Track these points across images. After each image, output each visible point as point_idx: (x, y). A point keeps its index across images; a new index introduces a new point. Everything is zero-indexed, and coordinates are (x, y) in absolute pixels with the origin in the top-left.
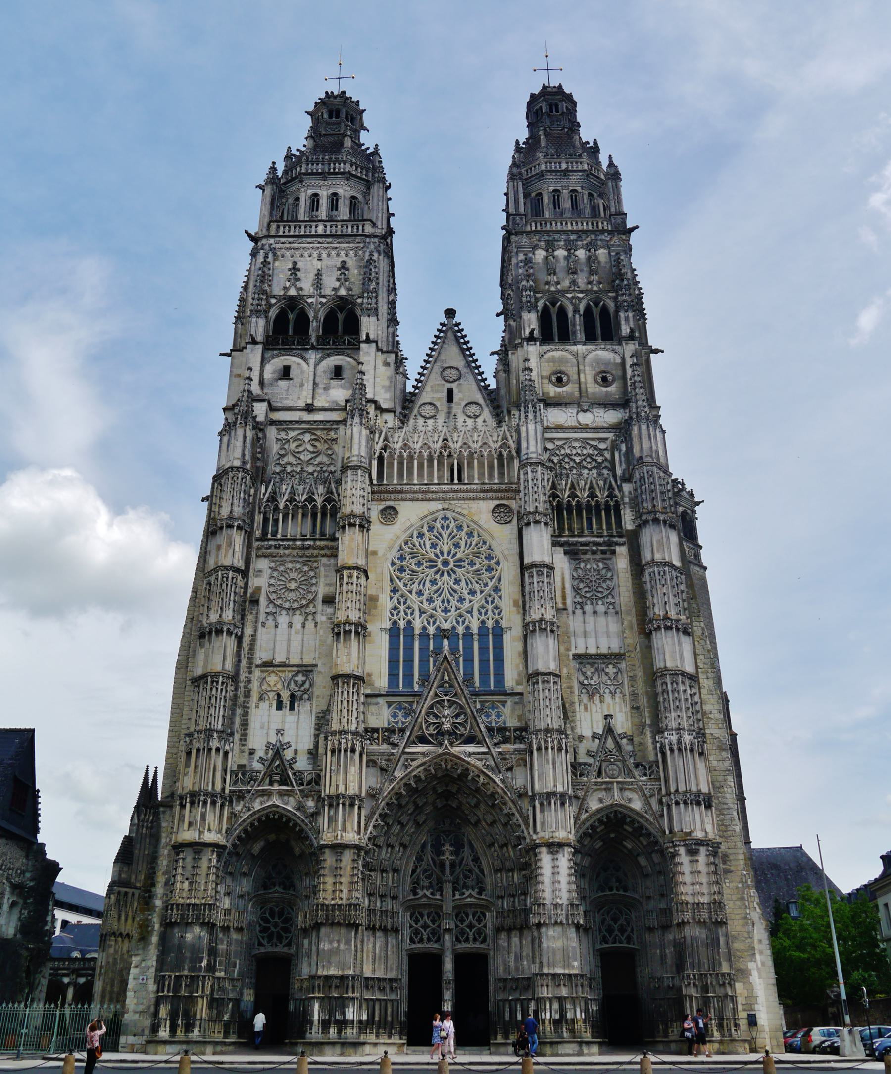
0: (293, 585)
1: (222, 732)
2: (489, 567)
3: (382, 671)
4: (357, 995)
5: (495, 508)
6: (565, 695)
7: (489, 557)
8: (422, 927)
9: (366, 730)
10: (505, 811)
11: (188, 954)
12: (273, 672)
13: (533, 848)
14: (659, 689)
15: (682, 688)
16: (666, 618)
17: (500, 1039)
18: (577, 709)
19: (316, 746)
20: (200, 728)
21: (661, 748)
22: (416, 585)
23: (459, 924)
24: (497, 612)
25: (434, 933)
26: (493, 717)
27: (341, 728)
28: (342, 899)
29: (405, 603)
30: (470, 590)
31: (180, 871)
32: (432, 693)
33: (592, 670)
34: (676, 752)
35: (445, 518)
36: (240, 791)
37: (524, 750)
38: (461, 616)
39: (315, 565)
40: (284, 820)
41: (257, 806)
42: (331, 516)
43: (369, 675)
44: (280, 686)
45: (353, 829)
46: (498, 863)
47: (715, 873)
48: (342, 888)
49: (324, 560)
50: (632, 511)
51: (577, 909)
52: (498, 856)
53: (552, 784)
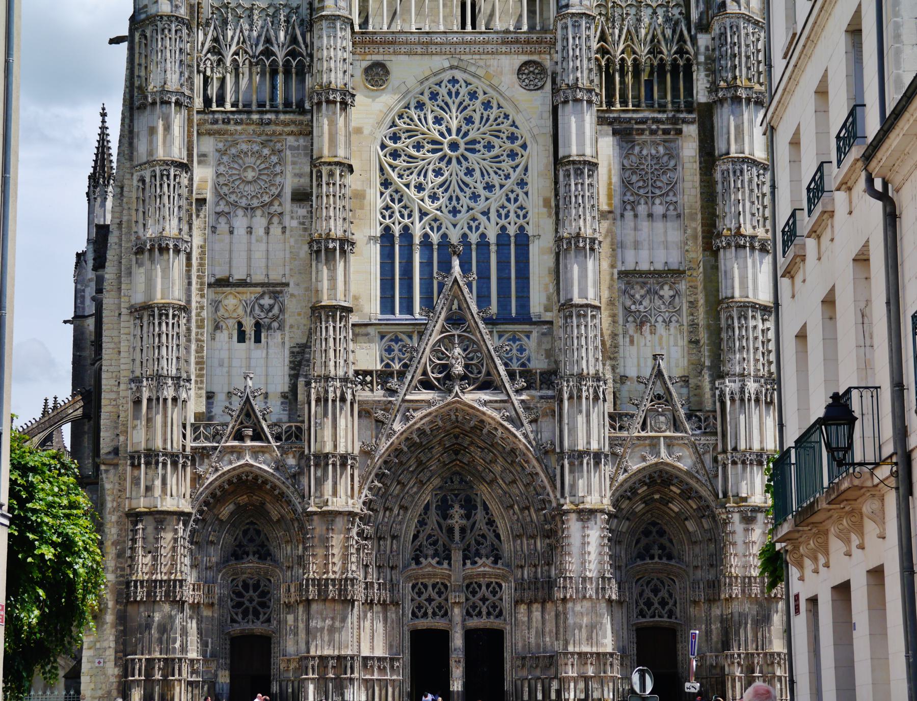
0: (250, 175)
2: (512, 151)
5: (521, 66)
7: (512, 138)
8: (426, 600)
9: (357, 373)
10: (528, 470)
14: (723, 323)
16: (738, 234)
18: (621, 343)
19: (294, 389)
21: (720, 396)
22: (414, 176)
23: (470, 596)
24: (521, 213)
25: (440, 607)
26: (514, 351)
27: (327, 373)
28: (334, 572)
29: (400, 201)
30: (487, 183)
34: (738, 402)
35: (454, 81)
36: (204, 448)
37: (553, 397)
38: (474, 219)
39: (278, 146)
40: (260, 481)
42: (297, 74)
44: (240, 311)
48: (336, 560)
49: (291, 140)
50: (707, 76)
52: (518, 520)
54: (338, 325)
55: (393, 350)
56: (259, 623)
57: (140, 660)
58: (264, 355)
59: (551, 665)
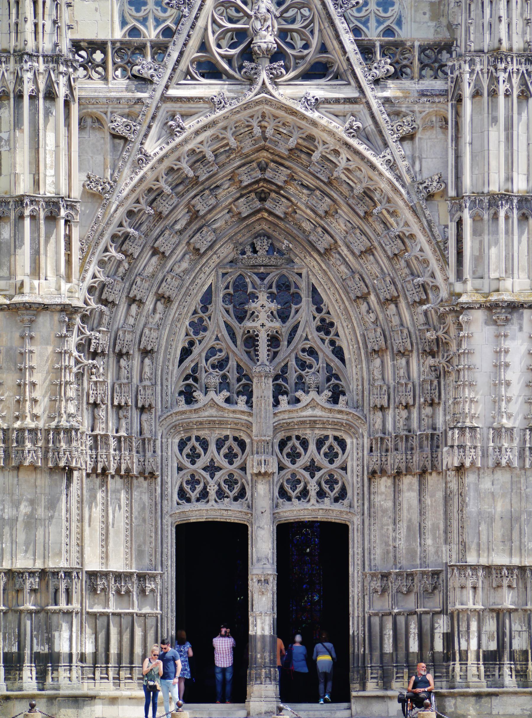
4: (75, 606)
9: (76, 46)
10: (397, 229)
23: (287, 462)
25: (231, 482)
27: (20, 46)
28: (35, 417)
37: (444, 93)
48: (37, 394)
52: (376, 322)
59: (435, 588)
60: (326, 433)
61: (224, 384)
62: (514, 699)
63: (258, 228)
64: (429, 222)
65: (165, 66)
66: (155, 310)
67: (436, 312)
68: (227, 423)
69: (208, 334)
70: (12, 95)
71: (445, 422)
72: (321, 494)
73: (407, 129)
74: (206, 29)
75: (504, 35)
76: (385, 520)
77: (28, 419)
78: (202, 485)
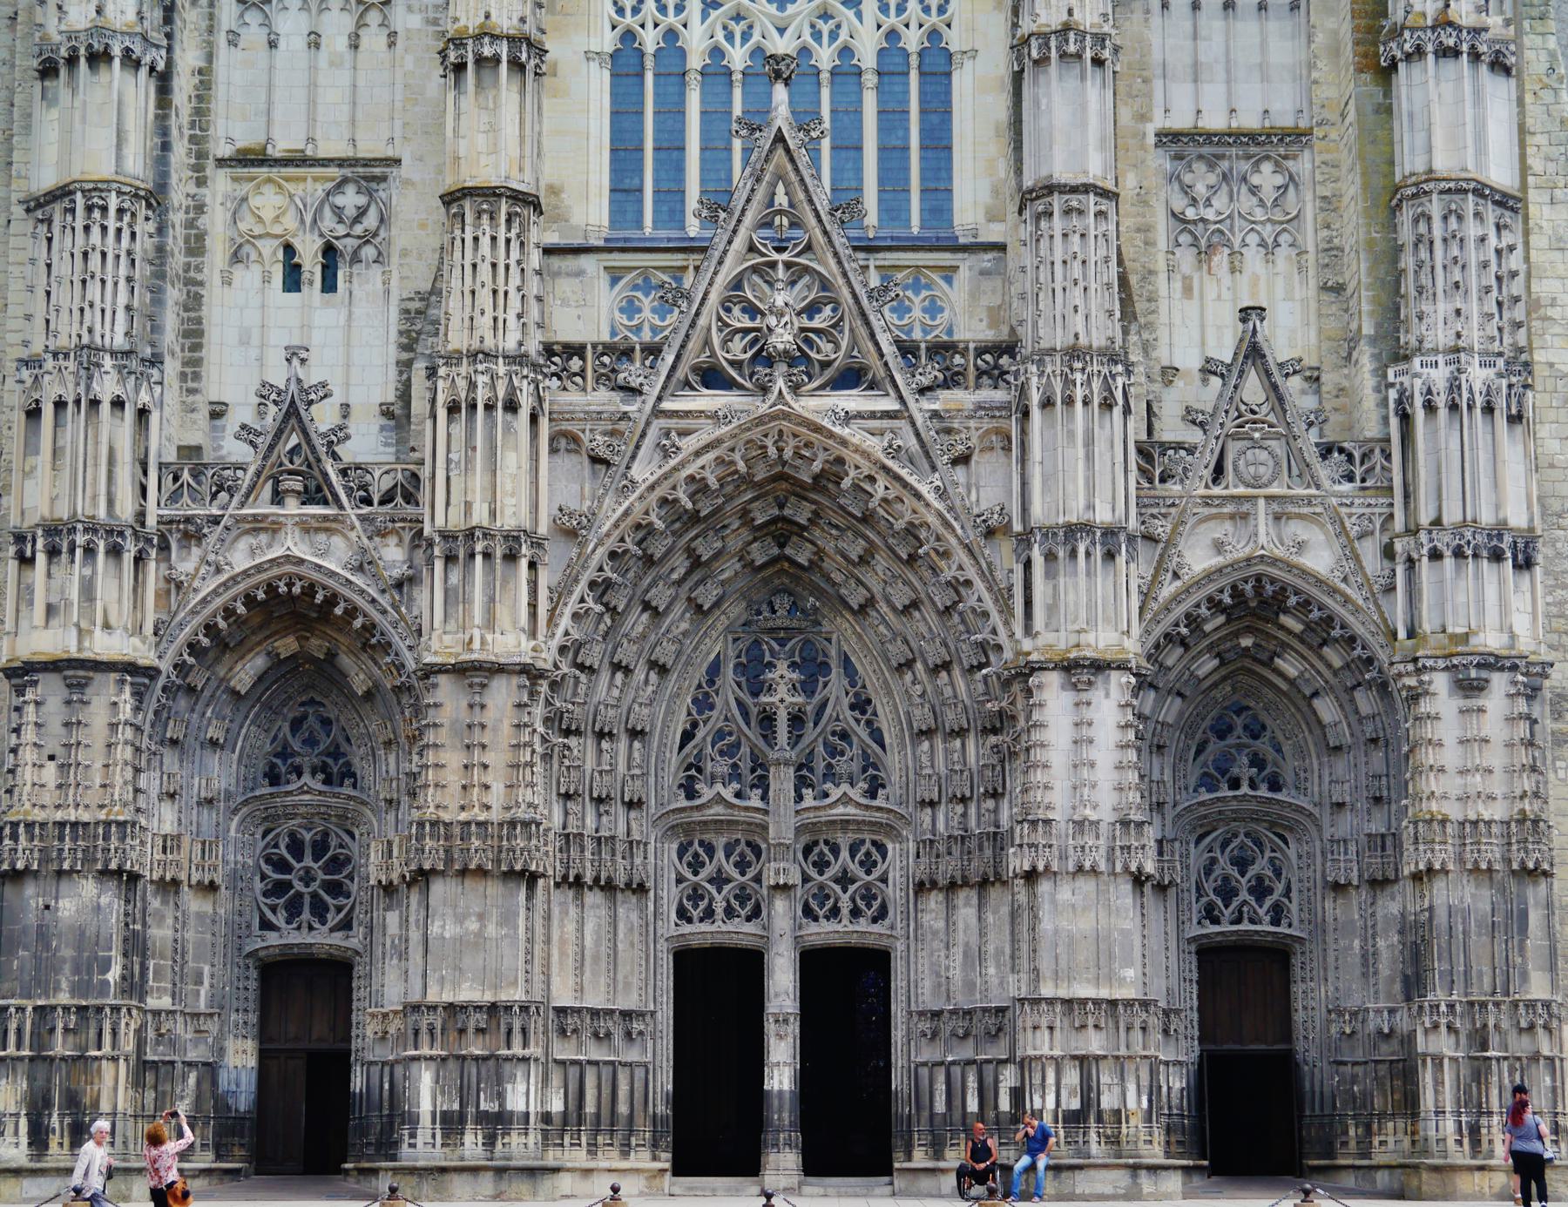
1: (127, 354)
3: (593, 178)
4: (535, 1050)
6: (1128, 253)
9: (549, 350)
10: (948, 574)
11: (67, 952)
12: (269, 180)
13: (1025, 672)
14: (1406, 234)
15: (1472, 230)
17: (920, 1158)
18: (1163, 291)
19: (405, 395)
20: (62, 342)
21: (1399, 402)
23: (813, 873)
25: (742, 898)
26: (917, 313)
27: (476, 345)
28: (488, 808)
31: (29, 735)
32: (739, 243)
33: (1212, 179)
34: (1443, 413)
36: (188, 520)
37: (1006, 407)
38: (826, 16)
40: (319, 598)
41: (240, 558)
43: (554, 190)
44: (290, 222)
45: (515, 622)
46: (922, 716)
47: (1530, 744)
48: (488, 778)
51: (1140, 834)
52: (923, 695)
53: (1082, 502)
54: (502, 235)
55: (639, 310)
56: (325, 929)
57: (21, 1009)
58: (342, 320)
59: (1000, 1029)
60: (860, 836)
61: (735, 775)
62: (1104, 1174)
63: (777, 582)
64: (989, 564)
65: (658, 374)
66: (647, 681)
67: (999, 678)
68: (737, 822)
69: (715, 713)
70: (463, 405)
71: (1011, 816)
72: (856, 913)
73: (960, 448)
74: (709, 329)
75: (1080, 329)
76: (936, 944)
77: (476, 810)
78: (706, 901)
